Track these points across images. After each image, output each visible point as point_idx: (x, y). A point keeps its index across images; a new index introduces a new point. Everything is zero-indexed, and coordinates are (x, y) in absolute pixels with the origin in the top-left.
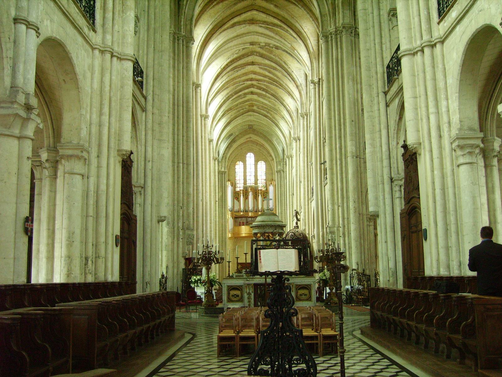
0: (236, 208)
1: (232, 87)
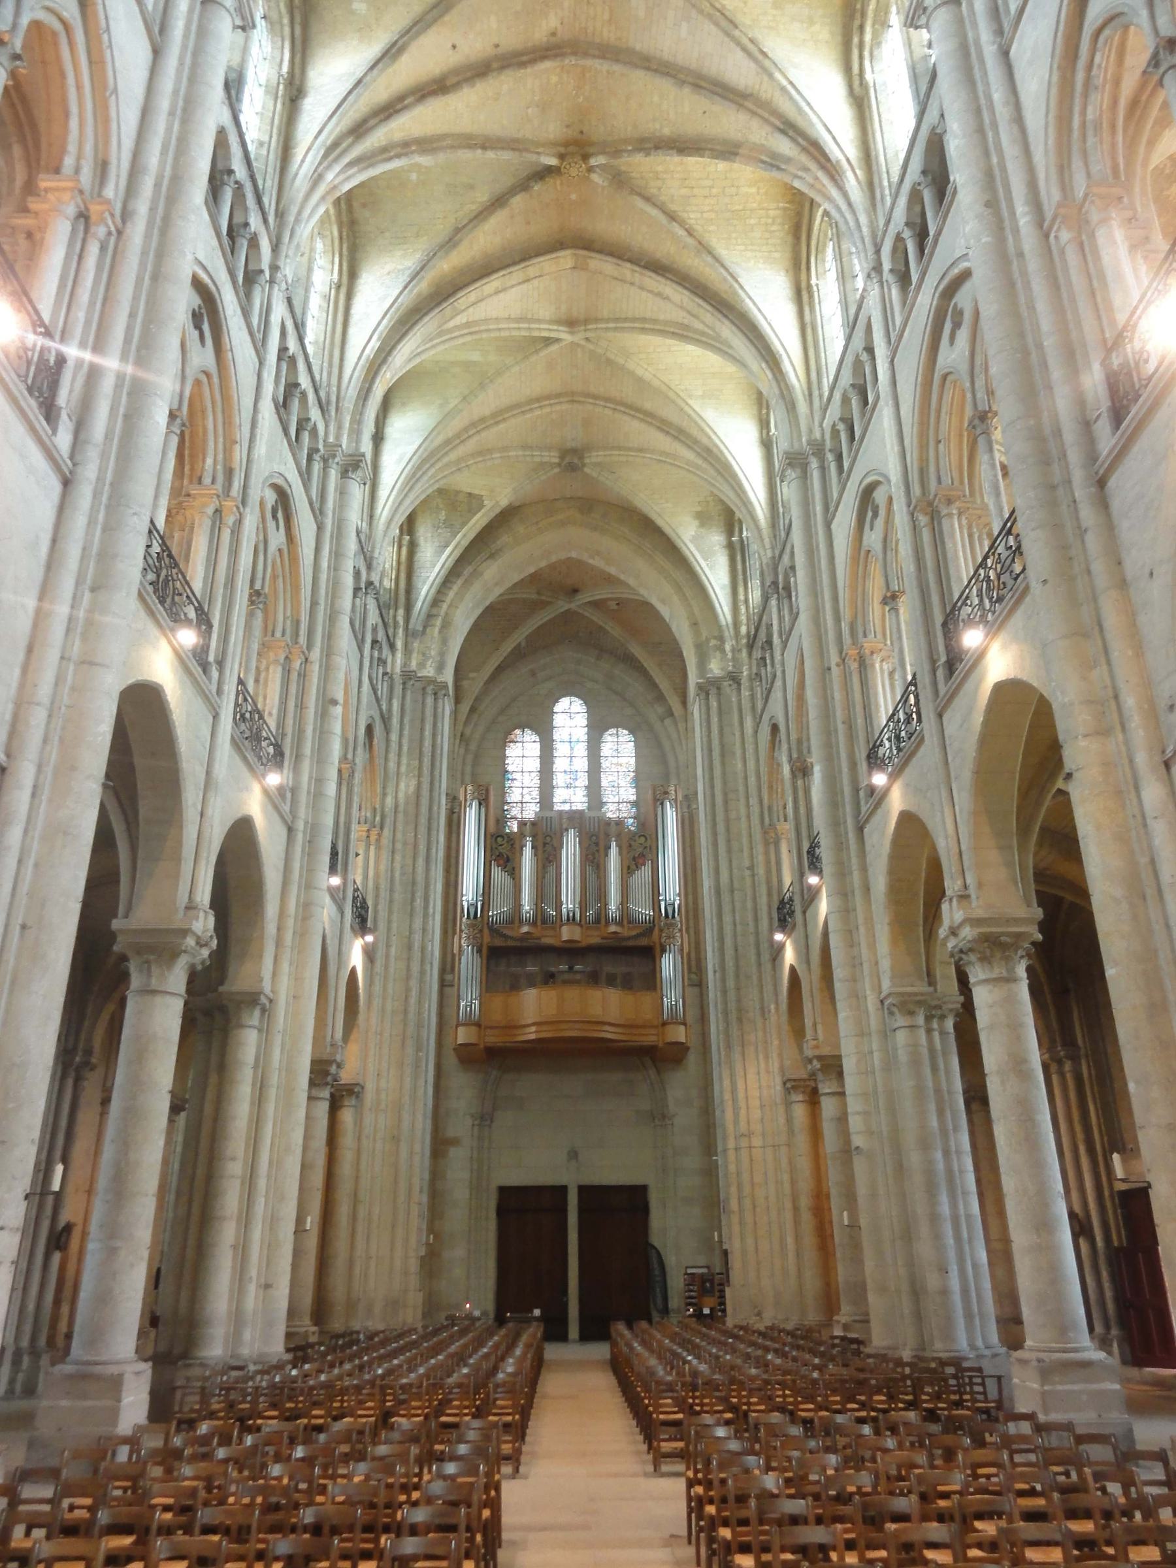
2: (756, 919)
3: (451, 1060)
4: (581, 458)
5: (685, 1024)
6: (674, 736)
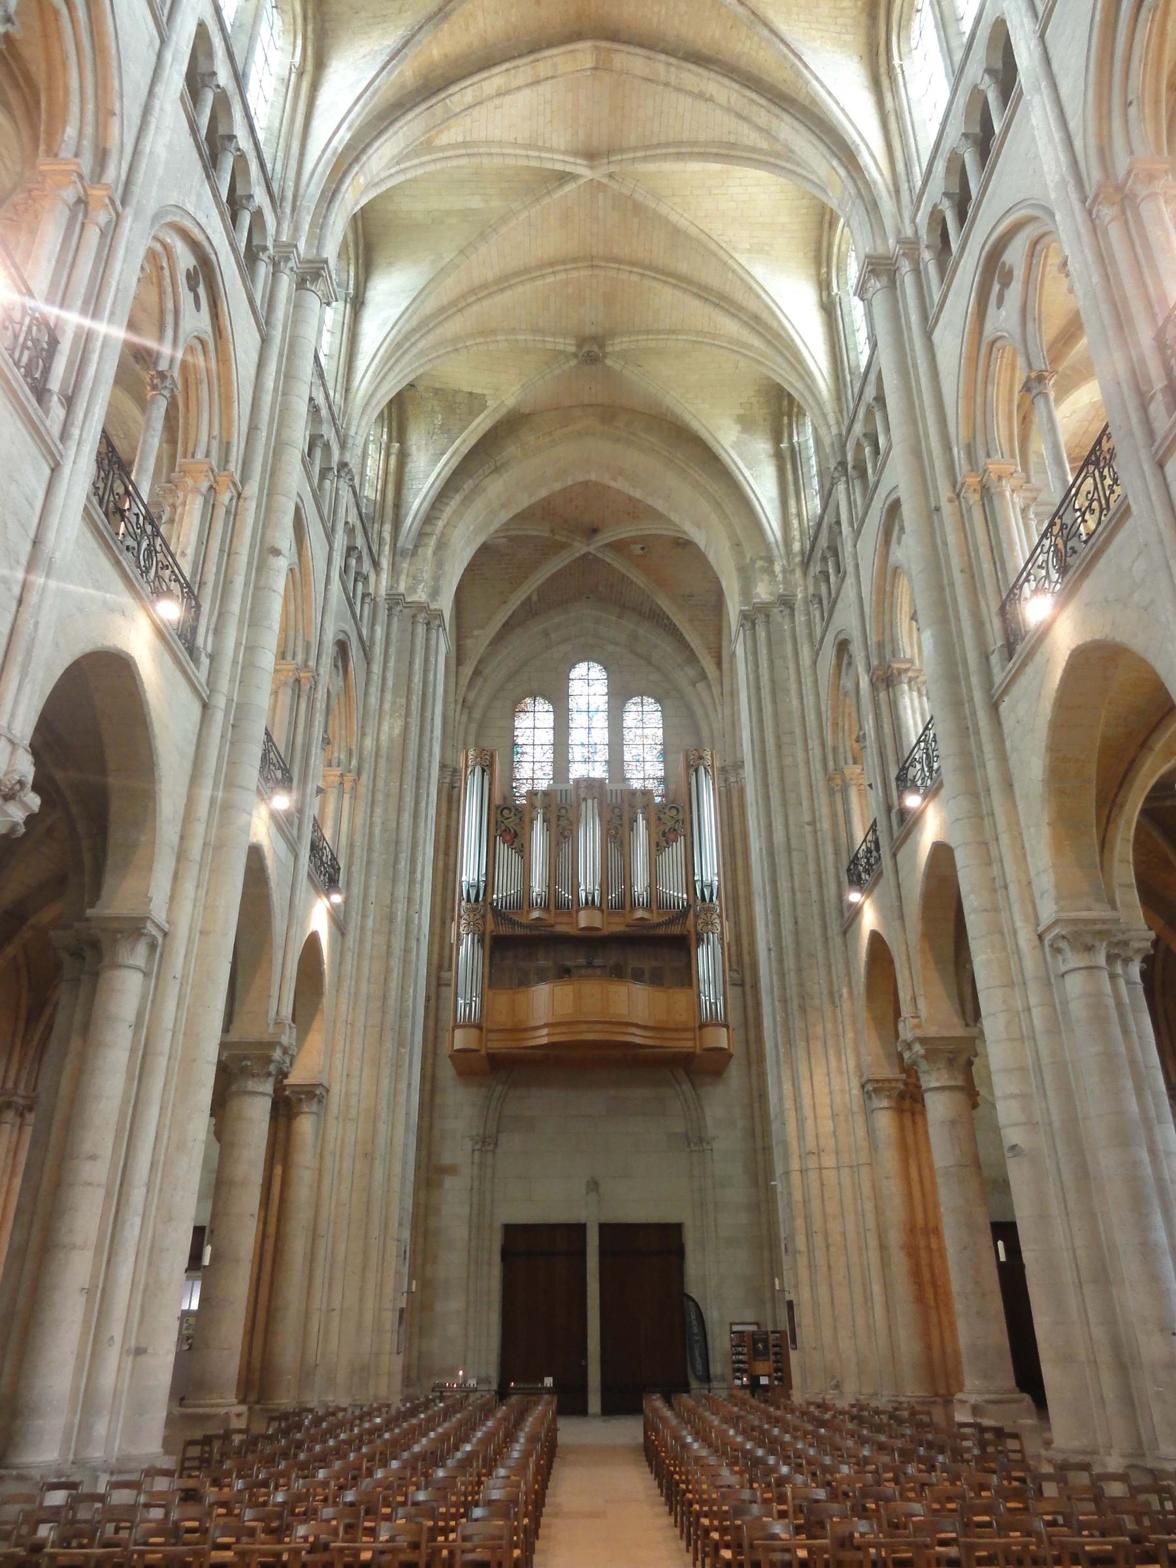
0: (505, 889)
2: (821, 885)
3: (447, 1071)
4: (602, 346)
5: (727, 1027)
6: (708, 701)
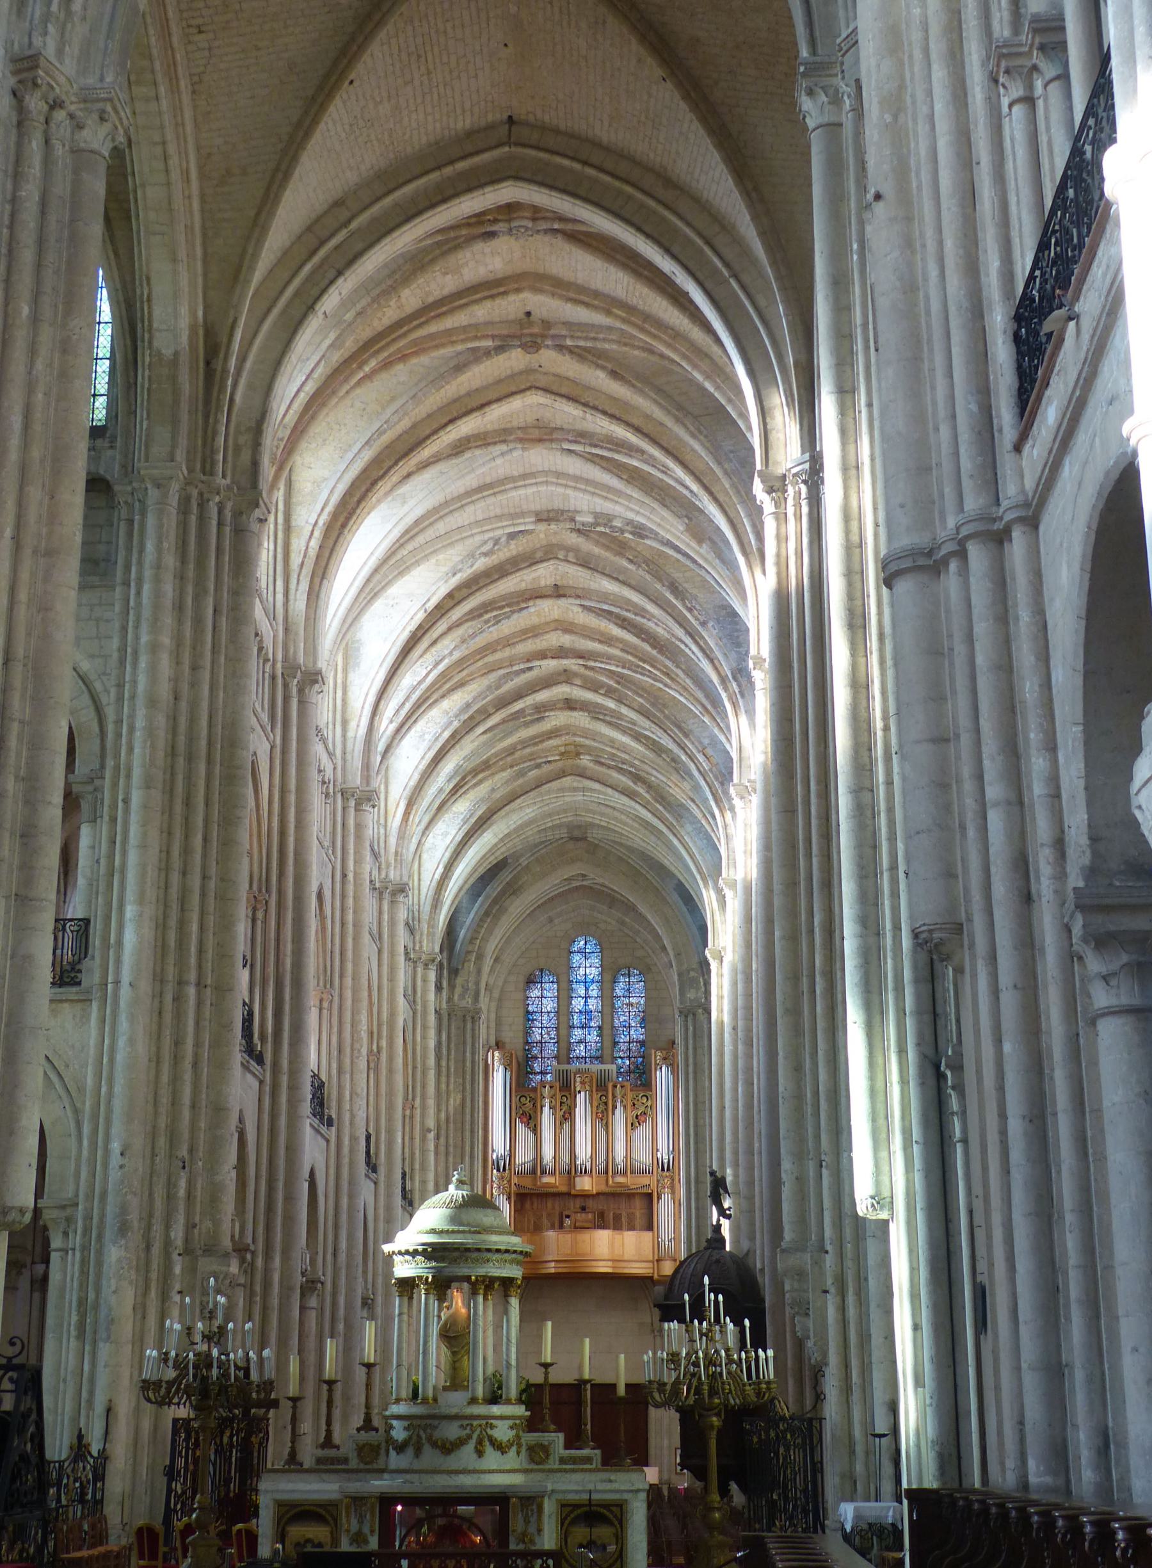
1: (486, 682)
